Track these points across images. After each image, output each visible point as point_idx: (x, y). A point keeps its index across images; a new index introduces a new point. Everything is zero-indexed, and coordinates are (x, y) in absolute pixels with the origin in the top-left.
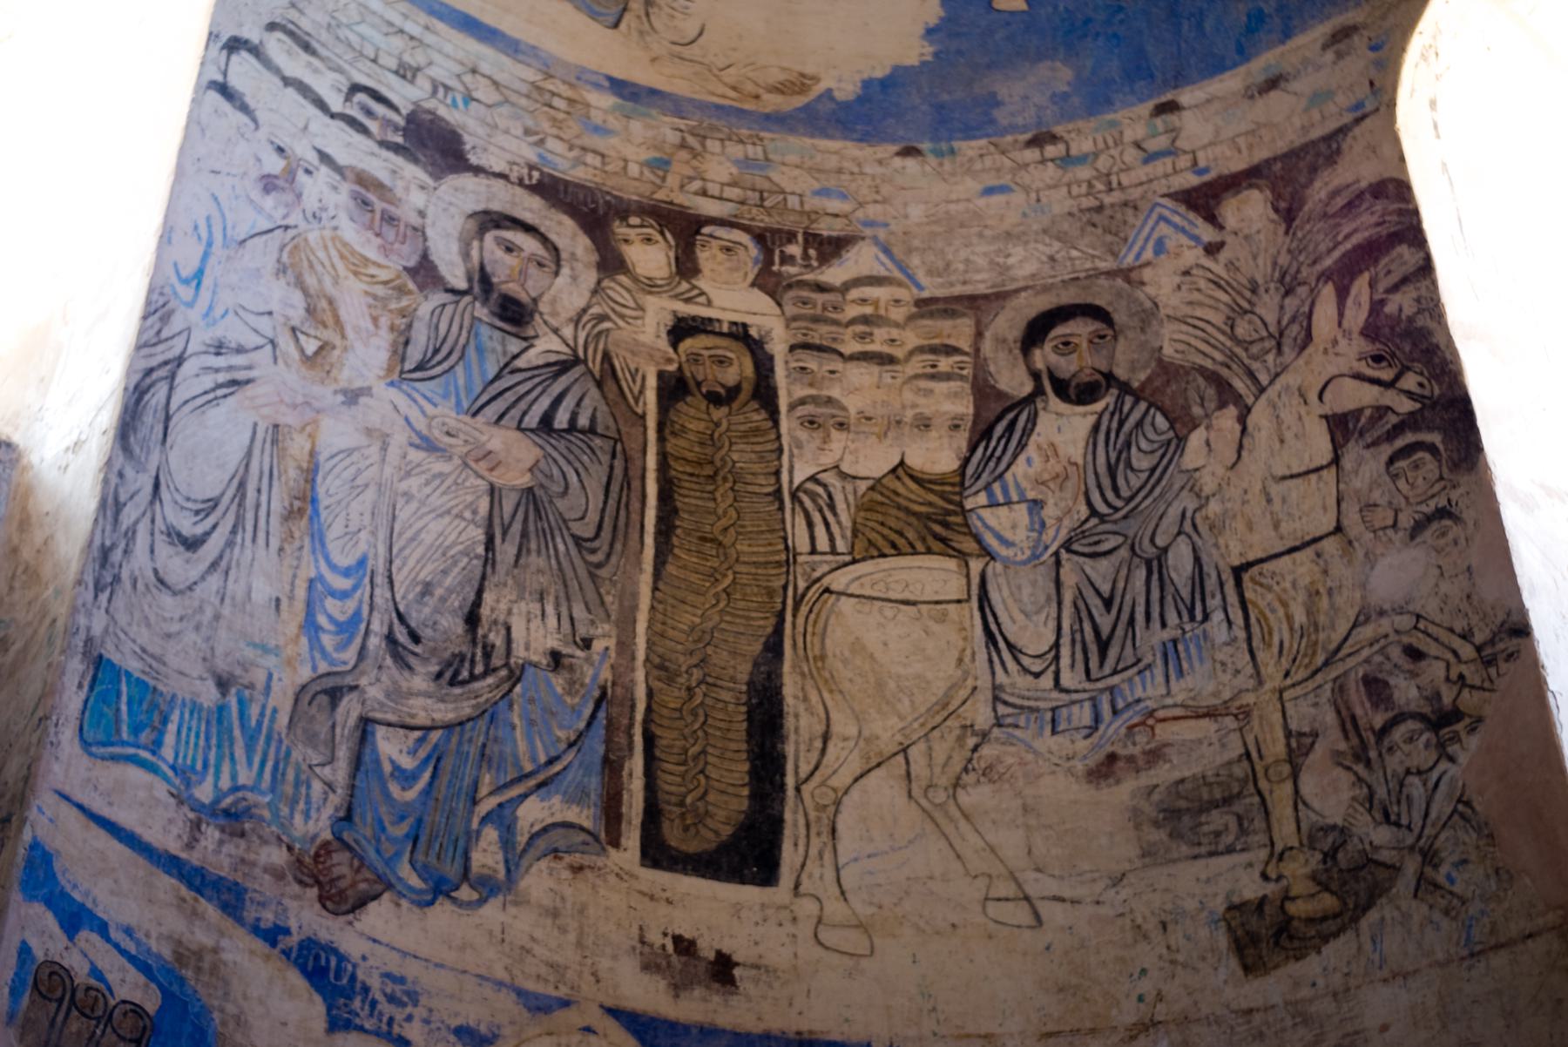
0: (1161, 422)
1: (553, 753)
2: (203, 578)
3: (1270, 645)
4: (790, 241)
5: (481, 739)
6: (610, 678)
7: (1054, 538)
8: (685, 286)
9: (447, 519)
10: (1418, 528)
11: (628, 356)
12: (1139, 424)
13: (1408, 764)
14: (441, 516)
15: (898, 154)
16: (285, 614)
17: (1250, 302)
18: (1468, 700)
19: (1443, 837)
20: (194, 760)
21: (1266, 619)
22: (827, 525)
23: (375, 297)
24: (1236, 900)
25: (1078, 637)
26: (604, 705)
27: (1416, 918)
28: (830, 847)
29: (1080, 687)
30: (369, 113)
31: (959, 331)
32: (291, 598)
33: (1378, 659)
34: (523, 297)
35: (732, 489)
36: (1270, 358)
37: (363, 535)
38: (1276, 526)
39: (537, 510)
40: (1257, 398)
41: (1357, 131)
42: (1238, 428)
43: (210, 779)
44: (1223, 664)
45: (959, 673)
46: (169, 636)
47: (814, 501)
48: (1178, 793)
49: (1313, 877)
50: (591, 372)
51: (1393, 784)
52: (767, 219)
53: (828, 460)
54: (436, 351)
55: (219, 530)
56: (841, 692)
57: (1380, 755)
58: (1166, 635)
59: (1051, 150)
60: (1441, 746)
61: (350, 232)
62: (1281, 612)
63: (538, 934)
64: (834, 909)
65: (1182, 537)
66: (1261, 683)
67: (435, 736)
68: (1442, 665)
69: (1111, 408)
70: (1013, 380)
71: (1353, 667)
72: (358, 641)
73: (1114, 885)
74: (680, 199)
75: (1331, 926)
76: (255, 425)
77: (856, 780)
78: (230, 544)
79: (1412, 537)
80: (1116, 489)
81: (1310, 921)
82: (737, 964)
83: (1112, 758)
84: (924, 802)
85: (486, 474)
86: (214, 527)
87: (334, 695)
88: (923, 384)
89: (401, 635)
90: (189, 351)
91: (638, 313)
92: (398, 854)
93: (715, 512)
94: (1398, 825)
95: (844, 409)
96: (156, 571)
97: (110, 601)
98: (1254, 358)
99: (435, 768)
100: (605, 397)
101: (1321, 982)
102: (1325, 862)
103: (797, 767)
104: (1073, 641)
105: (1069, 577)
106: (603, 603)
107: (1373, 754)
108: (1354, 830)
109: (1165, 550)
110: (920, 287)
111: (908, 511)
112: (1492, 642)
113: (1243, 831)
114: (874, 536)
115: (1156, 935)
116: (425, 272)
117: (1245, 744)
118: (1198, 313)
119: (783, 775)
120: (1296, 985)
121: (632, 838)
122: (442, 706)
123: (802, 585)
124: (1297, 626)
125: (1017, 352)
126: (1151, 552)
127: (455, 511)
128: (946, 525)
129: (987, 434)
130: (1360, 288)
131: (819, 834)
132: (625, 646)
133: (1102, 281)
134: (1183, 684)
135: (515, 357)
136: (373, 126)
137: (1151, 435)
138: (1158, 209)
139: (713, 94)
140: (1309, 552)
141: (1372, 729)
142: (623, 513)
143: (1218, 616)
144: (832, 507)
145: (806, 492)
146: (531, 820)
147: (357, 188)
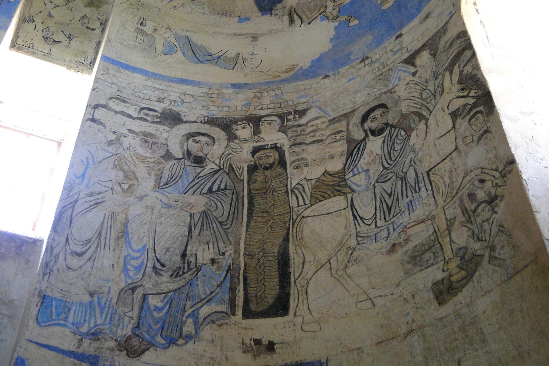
0: (403, 133)
1: (212, 290)
2: (85, 264)
3: (439, 193)
4: (289, 115)
5: (187, 292)
6: (232, 262)
7: (373, 180)
8: (256, 137)
9: (175, 227)
10: (480, 138)
11: (238, 163)
12: (397, 136)
13: (483, 219)
14: (173, 226)
15: (323, 79)
16: (116, 269)
17: (426, 86)
19: (496, 241)
20: (80, 320)
21: (437, 185)
22: (303, 197)
23: (149, 167)
24: (435, 281)
25: (382, 209)
26: (230, 271)
27: (490, 271)
28: (306, 298)
29: (383, 225)
30: (147, 115)
31: (342, 126)
32: (118, 263)
33: (472, 186)
34: (202, 155)
35: (272, 194)
36: (433, 101)
37: (144, 239)
38: (438, 154)
39: (207, 217)
40: (430, 115)
41: (451, 21)
42: (425, 126)
43: (86, 325)
44: (426, 204)
45: (346, 231)
46: (71, 284)
47: (298, 190)
48: (415, 250)
49: (458, 267)
50: (225, 171)
51: (479, 227)
52: (282, 110)
53: (302, 177)
54: (171, 178)
55: (91, 248)
56: (308, 247)
57: (475, 219)
58: (408, 200)
59: (367, 62)
60: (493, 209)
61: (140, 150)
62: (442, 181)
63: (207, 349)
64: (308, 317)
65: (411, 167)
67: (170, 294)
68: (490, 182)
69: (388, 134)
70: (358, 135)
71: (465, 192)
72: (143, 271)
73: (397, 287)
74: (254, 112)
75: (465, 281)
76: (105, 214)
77: (314, 274)
78: (95, 251)
79: (478, 143)
80: (391, 159)
81: (458, 281)
82: (276, 344)
83: (394, 245)
84: (336, 276)
85: (189, 210)
86: (89, 248)
87: (133, 290)
88: (332, 145)
89: (158, 266)
90: (80, 197)
91: (242, 149)
92: (156, 335)
93: (267, 203)
94: (482, 240)
95: (307, 160)
96: (67, 265)
97: (48, 278)
98: (428, 103)
99: (170, 304)
100: (230, 178)
101: (463, 302)
102: (461, 260)
103: (294, 275)
104: (380, 210)
105: (378, 191)
106: (229, 240)
107: (472, 219)
108: (469, 246)
109: (406, 173)
110: (330, 116)
111: (328, 185)
112: (504, 169)
113: (436, 257)
114: (317, 196)
115: (411, 300)
116: (168, 156)
117: (434, 228)
118: (412, 95)
119: (290, 279)
120: (456, 305)
121: (239, 312)
122: (172, 284)
123: (295, 217)
124: (447, 184)
125: (360, 126)
126: (402, 175)
127: (177, 225)
128: (340, 186)
129: (352, 154)
131: (302, 295)
132: (237, 251)
133: (384, 96)
134: (414, 214)
135: (199, 173)
136: (149, 118)
137: (400, 138)
138: (398, 68)
139: (265, 79)
140: (448, 159)
141: (472, 210)
142: (236, 211)
143: (423, 189)
144: (304, 191)
145: (295, 189)
146: (204, 313)
147: (143, 137)
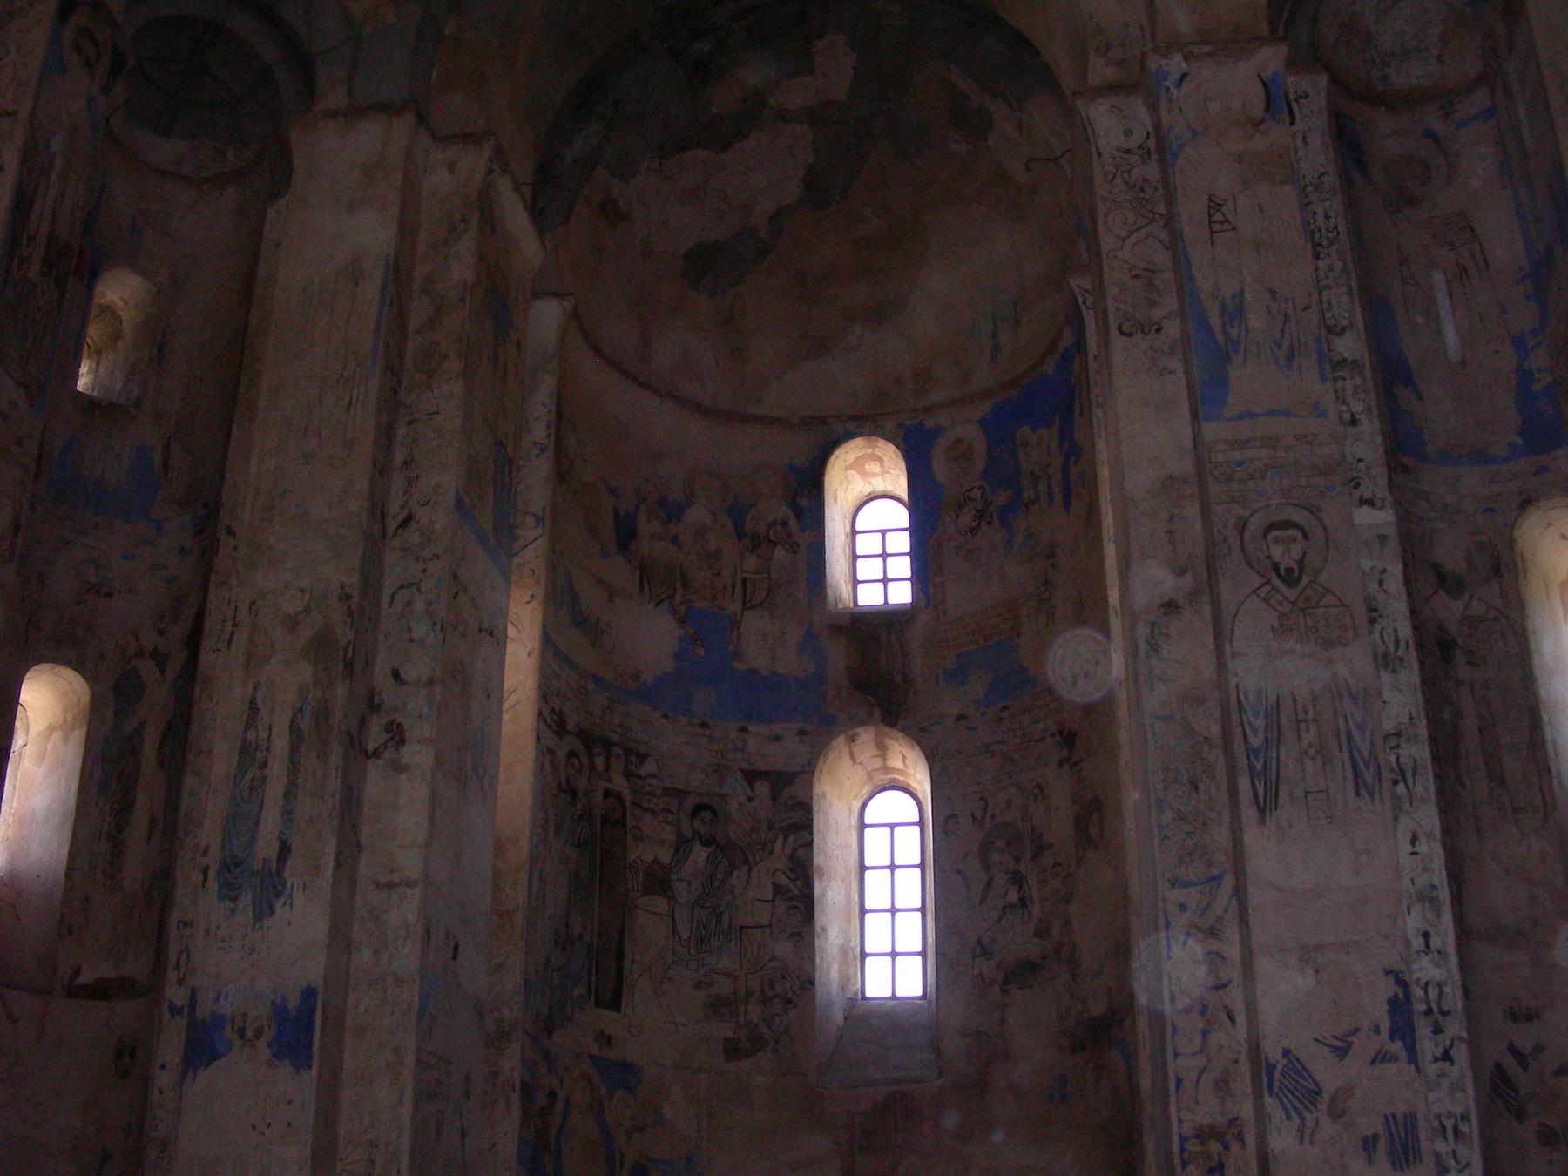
12: (720, 861)
18: (795, 998)
59: (707, 732)
66: (741, 969)
70: (687, 832)
79: (790, 938)
83: (700, 982)
105: (696, 915)
109: (722, 913)
116: (560, 785)
130: (791, 839)
143: (733, 942)
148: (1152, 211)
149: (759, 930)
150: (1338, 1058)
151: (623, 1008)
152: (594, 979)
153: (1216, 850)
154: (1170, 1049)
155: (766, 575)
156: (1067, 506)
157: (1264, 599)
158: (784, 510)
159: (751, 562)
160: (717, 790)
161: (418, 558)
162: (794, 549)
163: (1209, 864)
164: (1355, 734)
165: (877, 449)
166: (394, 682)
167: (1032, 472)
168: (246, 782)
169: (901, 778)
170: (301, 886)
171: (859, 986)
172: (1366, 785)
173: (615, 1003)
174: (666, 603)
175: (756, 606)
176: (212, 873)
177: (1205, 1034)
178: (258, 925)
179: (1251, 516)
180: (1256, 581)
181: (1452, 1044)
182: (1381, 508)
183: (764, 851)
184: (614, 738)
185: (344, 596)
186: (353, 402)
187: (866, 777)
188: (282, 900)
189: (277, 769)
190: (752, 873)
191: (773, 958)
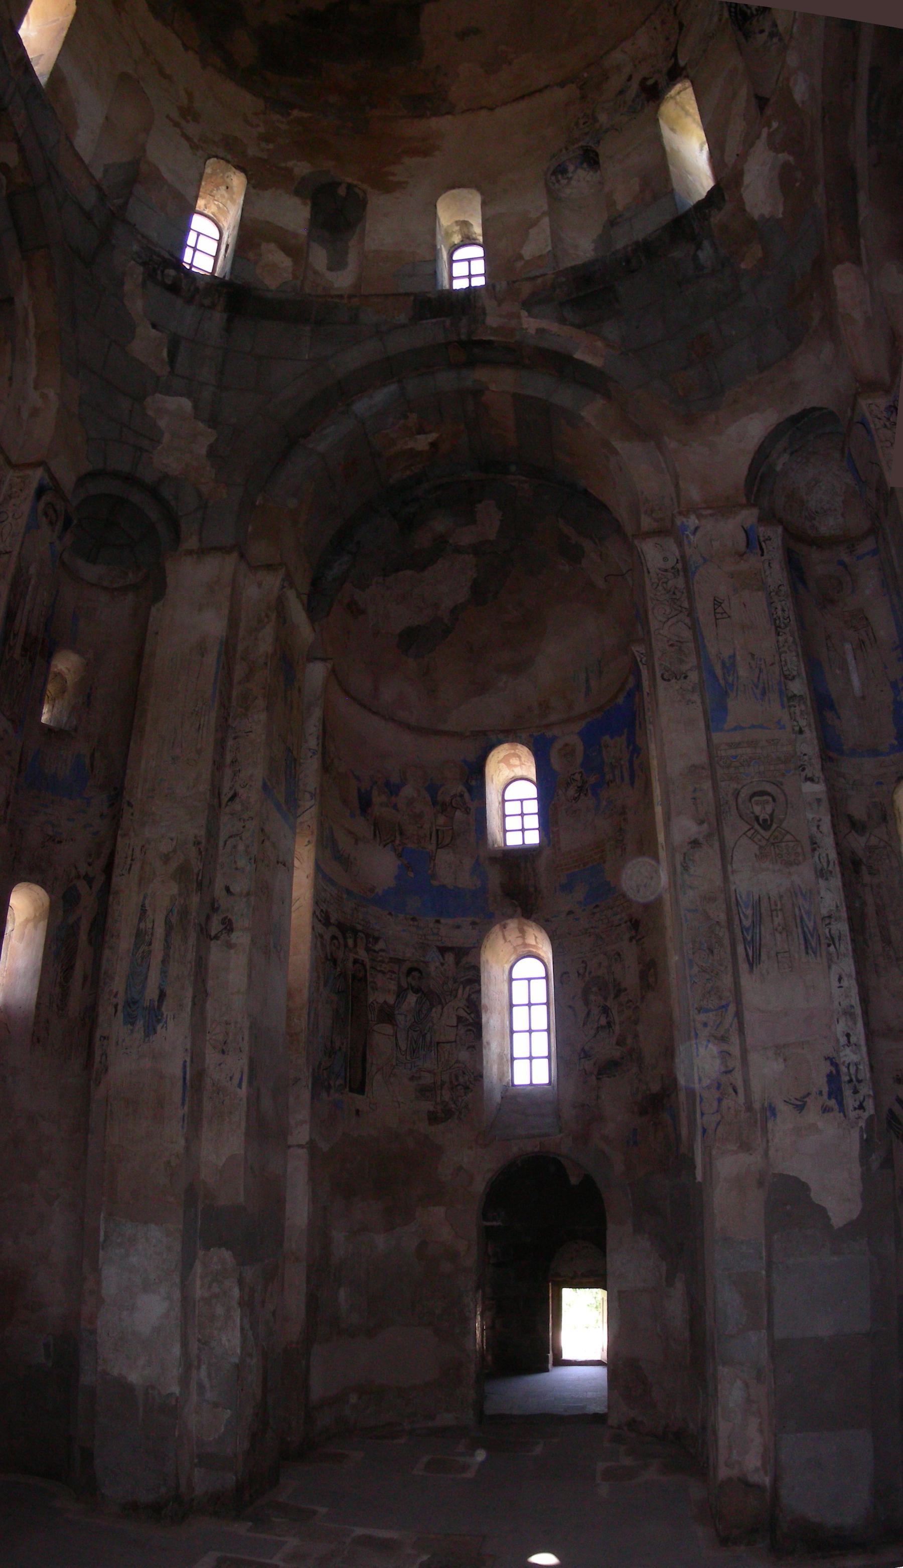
12: (424, 1003)
58: (424, 1053)
59: (416, 923)
66: (438, 1069)
70: (404, 984)
79: (467, 1049)
83: (413, 1076)
105: (410, 1036)
109: (426, 1034)
130: (467, 989)
143: (433, 1052)
148: (681, 606)
149: (449, 1044)
150: (799, 1112)
151: (366, 1093)
152: (348, 1075)
153: (724, 989)
154: (698, 1111)
155: (451, 827)
156: (632, 783)
157: (750, 838)
158: (461, 788)
159: (441, 820)
160: (422, 959)
161: (240, 819)
162: (467, 811)
163: (720, 998)
164: (805, 916)
165: (517, 750)
166: (226, 893)
167: (611, 763)
168: (139, 954)
169: (534, 950)
170: (173, 1017)
171: (510, 1078)
172: (812, 948)
173: (361, 1090)
174: (390, 845)
175: (444, 846)
176: (120, 1008)
177: (720, 1101)
178: (147, 1039)
179: (742, 788)
180: (746, 827)
181: (864, 1099)
182: (818, 783)
183: (451, 997)
184: (359, 927)
185: (196, 842)
186: (201, 726)
187: (513, 950)
188: (161, 1025)
189: (158, 946)
190: (444, 1009)
191: (457, 1061)
